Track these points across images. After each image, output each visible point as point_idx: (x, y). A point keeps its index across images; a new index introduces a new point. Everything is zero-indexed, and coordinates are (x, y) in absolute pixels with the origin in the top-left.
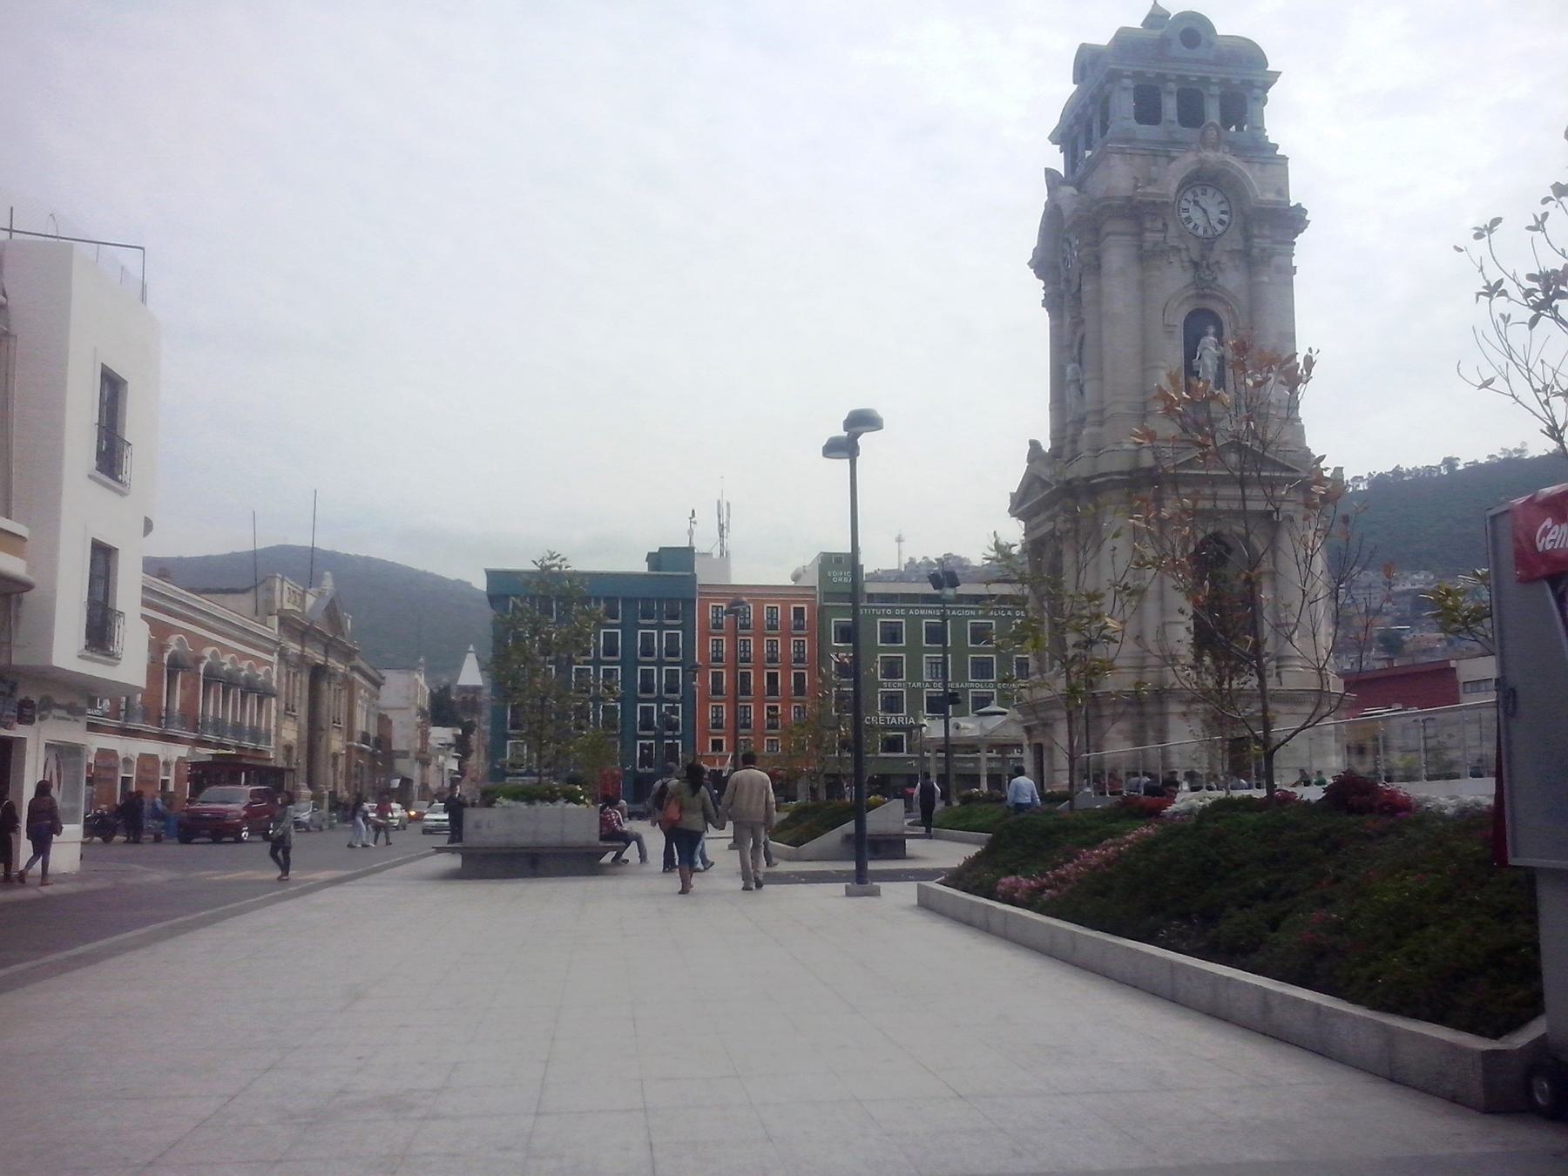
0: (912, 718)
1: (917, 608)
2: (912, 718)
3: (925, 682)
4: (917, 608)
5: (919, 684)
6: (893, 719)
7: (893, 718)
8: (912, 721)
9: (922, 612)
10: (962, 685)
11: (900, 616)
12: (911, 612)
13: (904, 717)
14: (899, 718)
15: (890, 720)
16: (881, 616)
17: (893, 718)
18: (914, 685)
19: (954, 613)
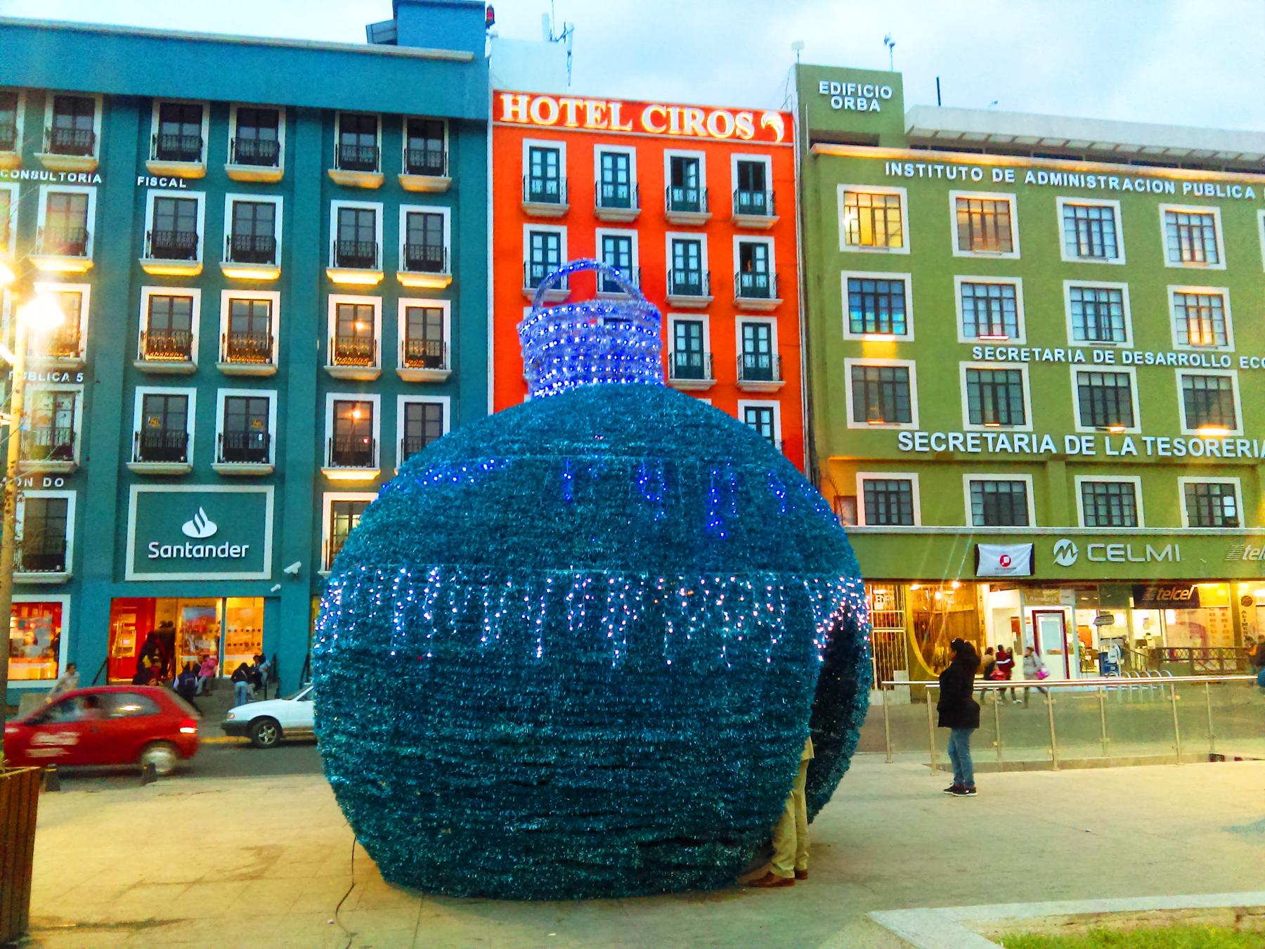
0: (1047, 438)
1: (1044, 169)
2: (1047, 438)
3: (1074, 349)
4: (1044, 169)
5: (1059, 354)
6: (1001, 439)
7: (1003, 437)
8: (1048, 444)
9: (1055, 179)
10: (1160, 358)
11: (1004, 186)
12: (1030, 177)
13: (1029, 434)
14: (1016, 437)
15: (995, 440)
16: (955, 184)
17: (1003, 437)
18: (1047, 355)
19: (1127, 184)
